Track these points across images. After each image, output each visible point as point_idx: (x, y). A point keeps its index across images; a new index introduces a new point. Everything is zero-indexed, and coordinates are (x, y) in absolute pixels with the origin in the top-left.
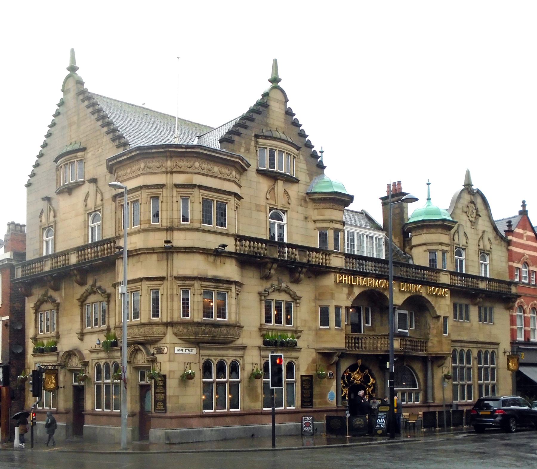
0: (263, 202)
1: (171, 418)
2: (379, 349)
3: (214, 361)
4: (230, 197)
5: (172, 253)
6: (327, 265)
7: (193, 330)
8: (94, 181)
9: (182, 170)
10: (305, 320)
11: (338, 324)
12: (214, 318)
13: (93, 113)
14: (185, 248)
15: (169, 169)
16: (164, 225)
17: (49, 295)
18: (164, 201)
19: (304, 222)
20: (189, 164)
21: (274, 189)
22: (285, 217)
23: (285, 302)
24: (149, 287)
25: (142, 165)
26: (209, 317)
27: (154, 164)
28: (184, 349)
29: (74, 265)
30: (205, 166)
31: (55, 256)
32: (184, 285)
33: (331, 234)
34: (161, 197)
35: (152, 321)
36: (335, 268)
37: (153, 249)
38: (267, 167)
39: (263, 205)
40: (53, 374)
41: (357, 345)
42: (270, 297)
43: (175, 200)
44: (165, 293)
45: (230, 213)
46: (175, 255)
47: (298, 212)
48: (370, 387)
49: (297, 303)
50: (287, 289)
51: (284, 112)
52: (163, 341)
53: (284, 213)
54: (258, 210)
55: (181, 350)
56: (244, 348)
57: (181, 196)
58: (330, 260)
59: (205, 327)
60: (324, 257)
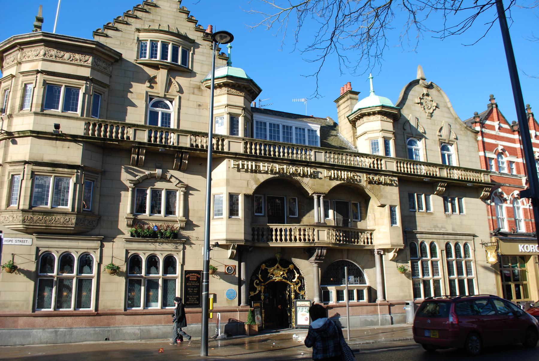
19: (197, 110)
28: (14, 239)
55: (10, 241)
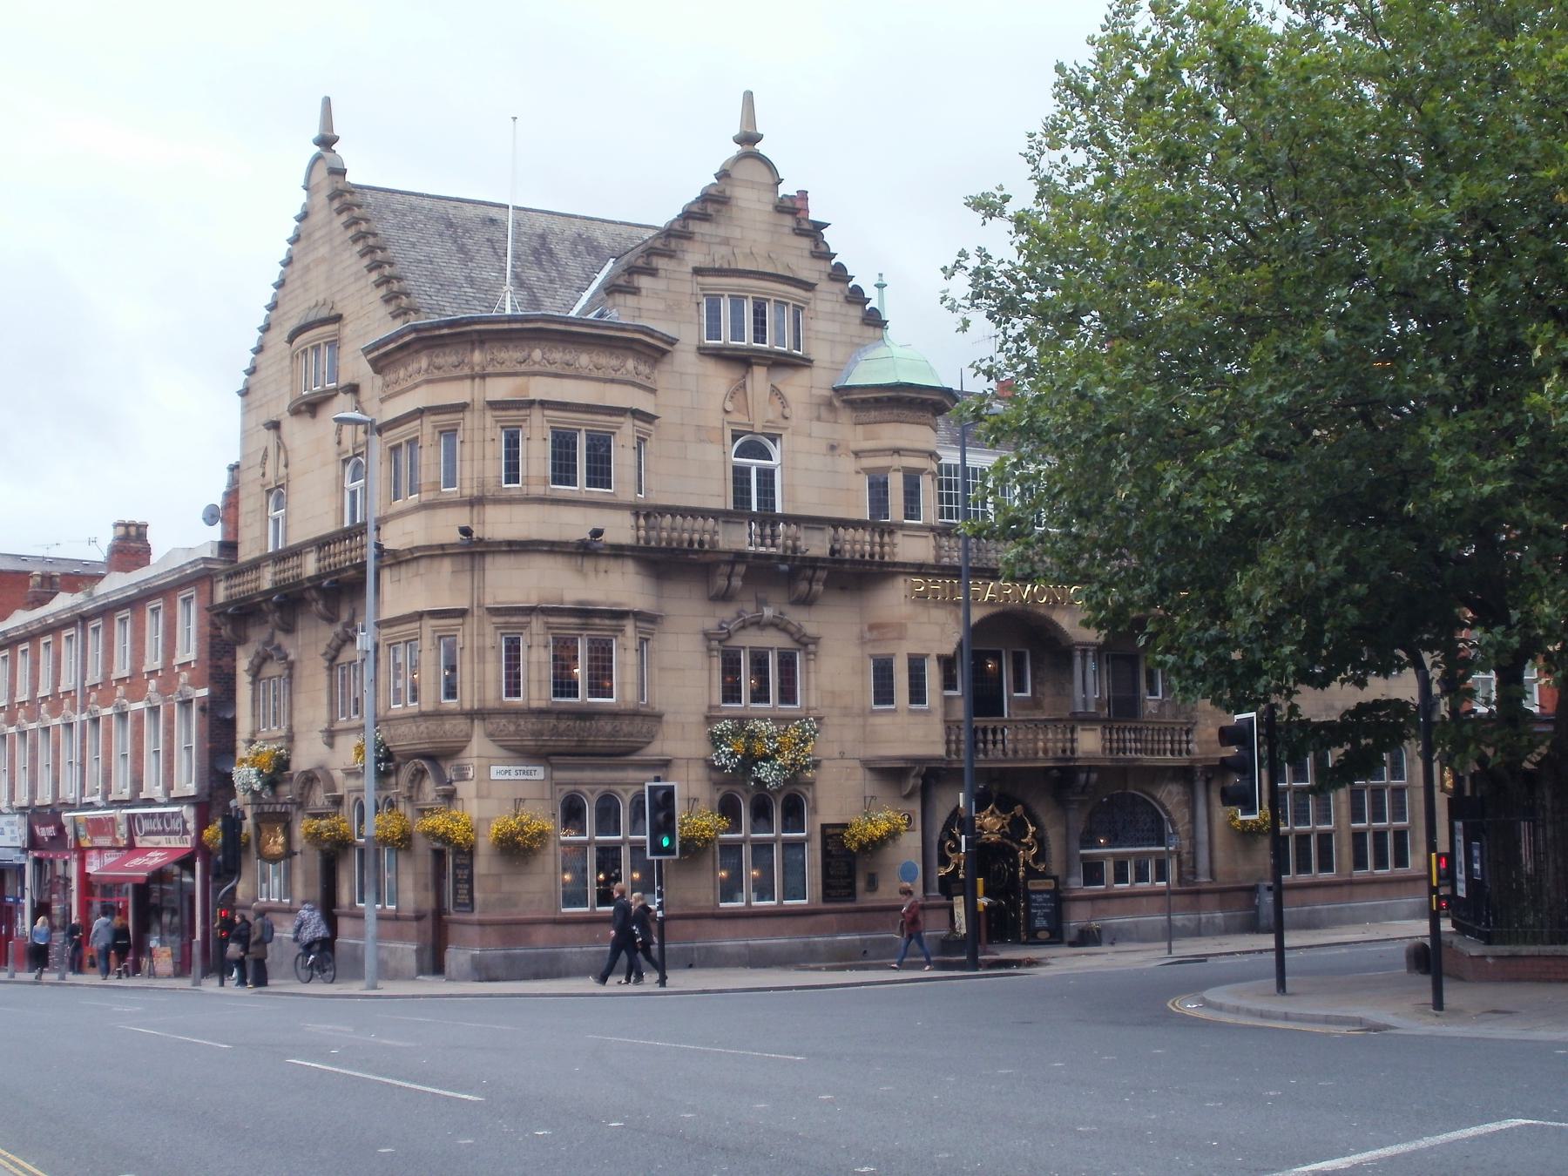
0: (714, 419)
1: (481, 924)
2: (1041, 754)
3: (588, 794)
4: (621, 419)
5: (483, 554)
6: (887, 558)
7: (530, 726)
8: (354, 389)
9: (504, 369)
10: (833, 693)
11: (917, 694)
12: (583, 698)
13: (355, 240)
14: (510, 543)
15: (477, 369)
16: (467, 492)
17: (276, 642)
18: (467, 439)
20: (518, 355)
21: (744, 386)
22: (776, 452)
23: (776, 652)
24: (435, 631)
25: (424, 363)
26: (569, 696)
27: (447, 359)
29: (310, 579)
30: (557, 356)
31: (280, 557)
32: (506, 626)
33: (896, 484)
34: (460, 433)
35: (442, 708)
36: (904, 565)
37: (442, 547)
38: (726, 339)
39: (714, 428)
40: (279, 821)
41: (981, 745)
42: (737, 641)
43: (489, 435)
44: (468, 645)
45: (622, 459)
46: (489, 560)
47: (810, 436)
48: (1030, 848)
49: (808, 653)
50: (778, 621)
51: (770, 208)
52: (466, 753)
53: (774, 441)
54: (701, 441)
56: (666, 764)
57: (502, 427)
58: (895, 545)
59: (558, 718)
60: (877, 539)
